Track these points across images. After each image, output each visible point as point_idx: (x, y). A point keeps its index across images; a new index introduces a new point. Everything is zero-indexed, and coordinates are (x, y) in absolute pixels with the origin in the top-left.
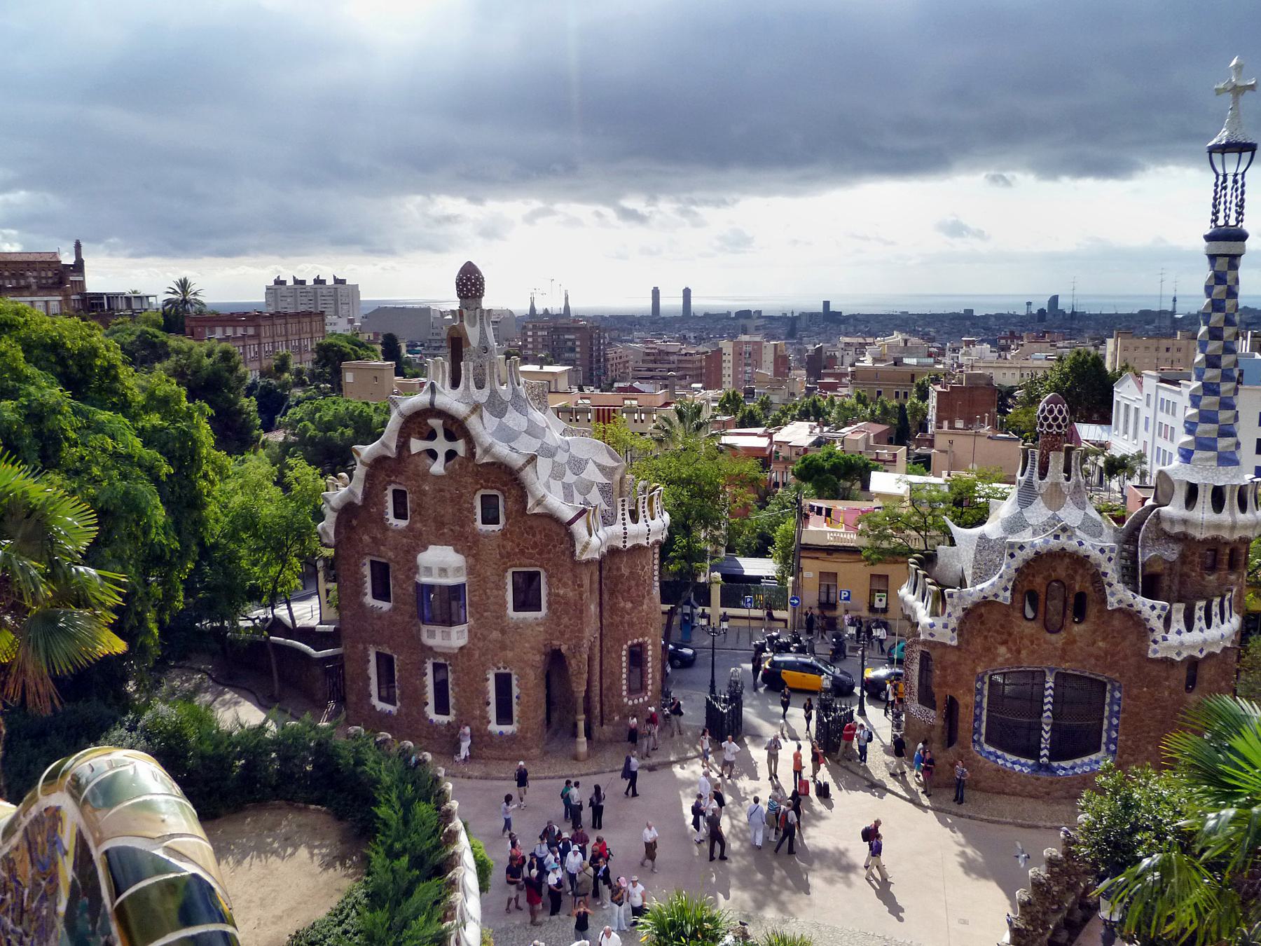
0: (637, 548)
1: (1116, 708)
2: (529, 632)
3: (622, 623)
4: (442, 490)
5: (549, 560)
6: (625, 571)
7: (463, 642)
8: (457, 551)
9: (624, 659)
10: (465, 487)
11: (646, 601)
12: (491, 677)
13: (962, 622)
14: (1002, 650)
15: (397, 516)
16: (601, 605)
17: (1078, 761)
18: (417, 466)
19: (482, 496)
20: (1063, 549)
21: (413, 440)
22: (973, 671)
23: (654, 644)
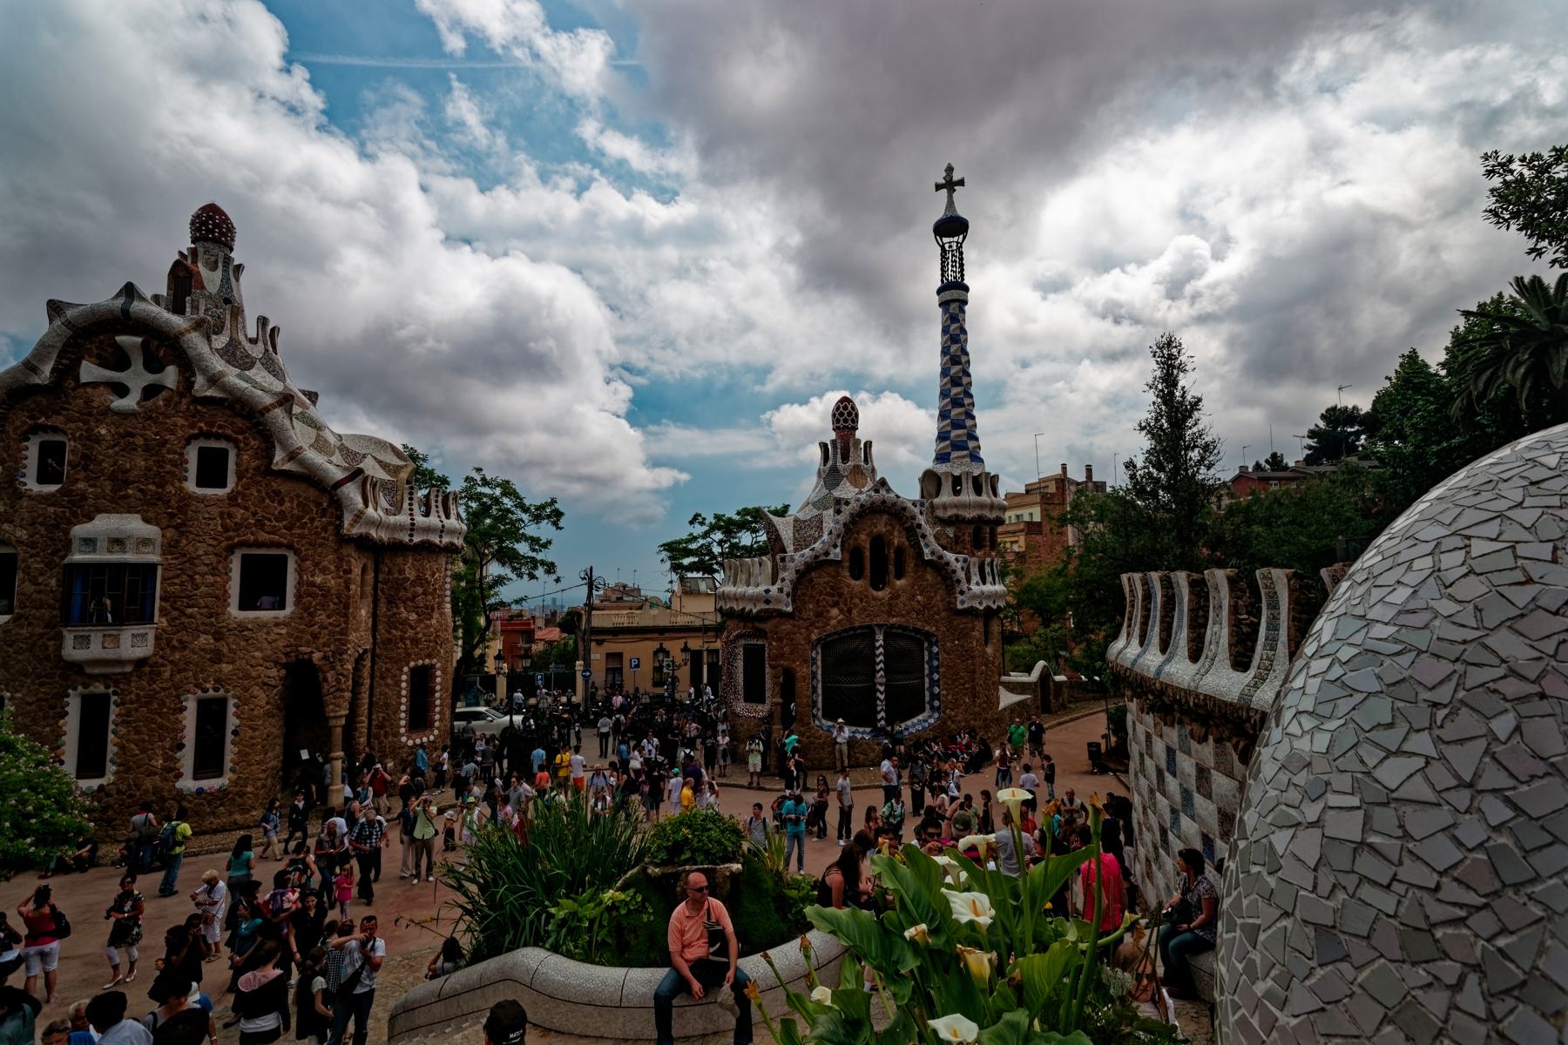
0: (427, 549)
1: (935, 663)
2: (262, 635)
3: (402, 639)
4: (132, 435)
5: (302, 537)
6: (410, 574)
7: (140, 652)
8: (147, 520)
9: (404, 685)
10: (172, 432)
11: (436, 615)
12: (191, 705)
13: (796, 584)
14: (835, 612)
15: (41, 480)
16: (374, 615)
17: (909, 723)
18: (88, 402)
19: (201, 450)
20: (884, 502)
21: (84, 363)
22: (808, 638)
23: (444, 671)
